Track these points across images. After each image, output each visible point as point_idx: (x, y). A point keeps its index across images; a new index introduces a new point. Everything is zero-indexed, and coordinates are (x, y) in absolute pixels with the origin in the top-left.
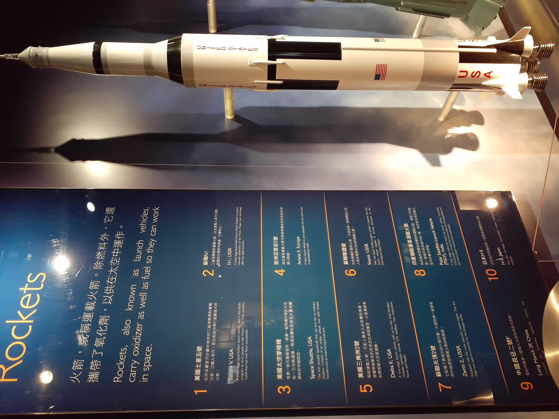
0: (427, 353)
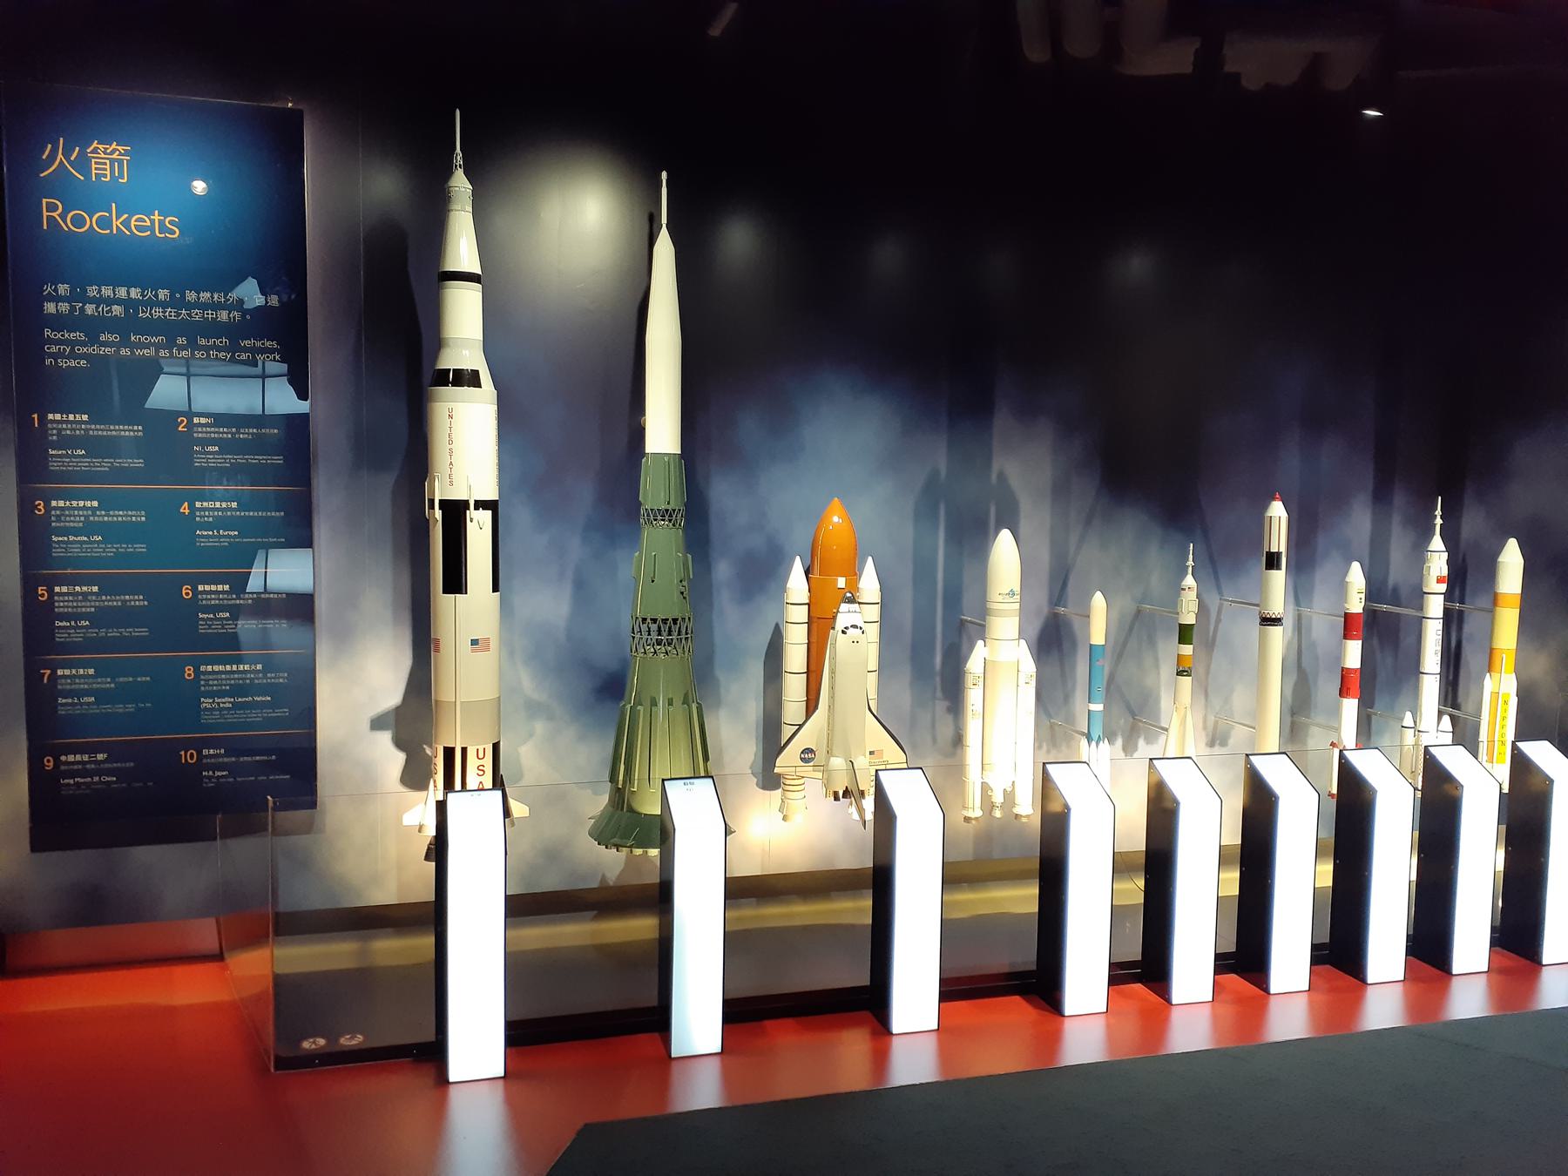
0: (85, 664)
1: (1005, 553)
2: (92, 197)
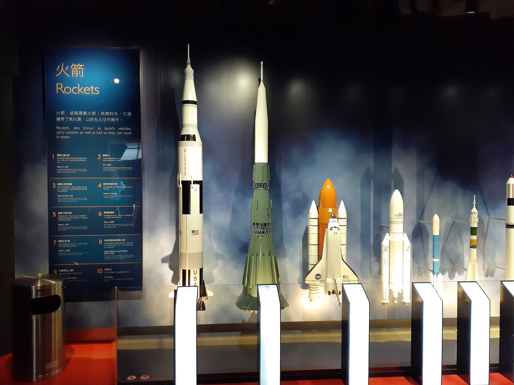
1: (397, 199)
2: (71, 82)
